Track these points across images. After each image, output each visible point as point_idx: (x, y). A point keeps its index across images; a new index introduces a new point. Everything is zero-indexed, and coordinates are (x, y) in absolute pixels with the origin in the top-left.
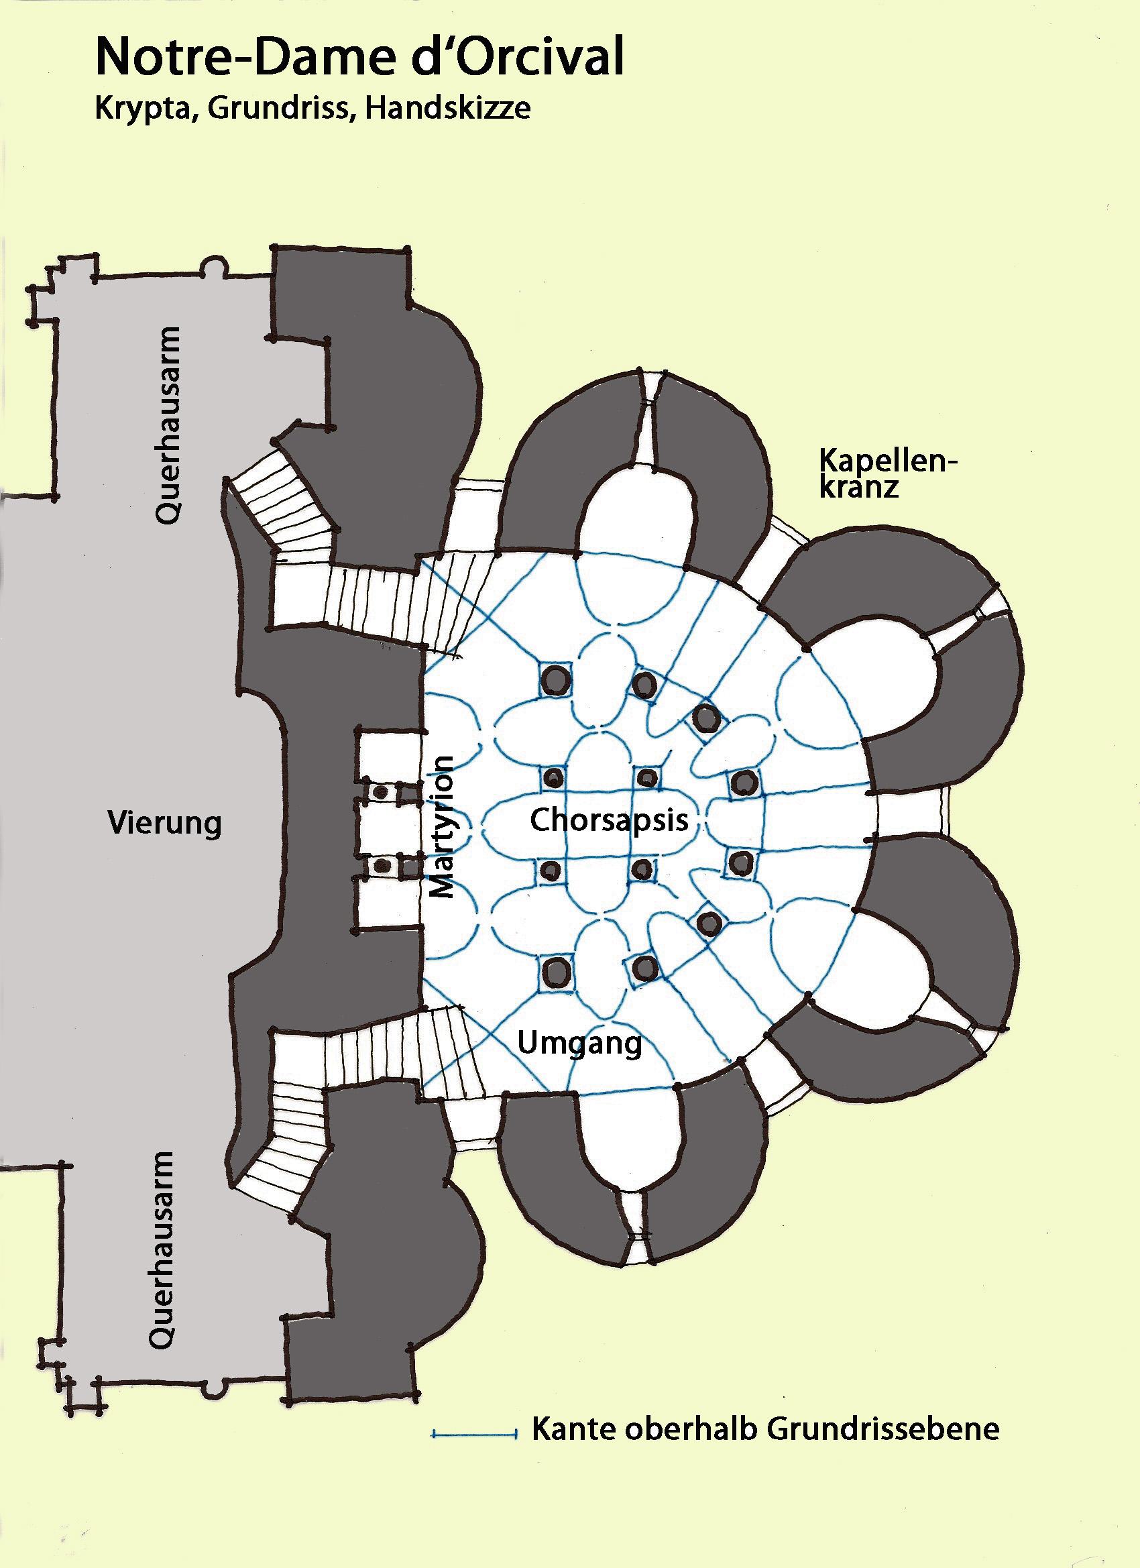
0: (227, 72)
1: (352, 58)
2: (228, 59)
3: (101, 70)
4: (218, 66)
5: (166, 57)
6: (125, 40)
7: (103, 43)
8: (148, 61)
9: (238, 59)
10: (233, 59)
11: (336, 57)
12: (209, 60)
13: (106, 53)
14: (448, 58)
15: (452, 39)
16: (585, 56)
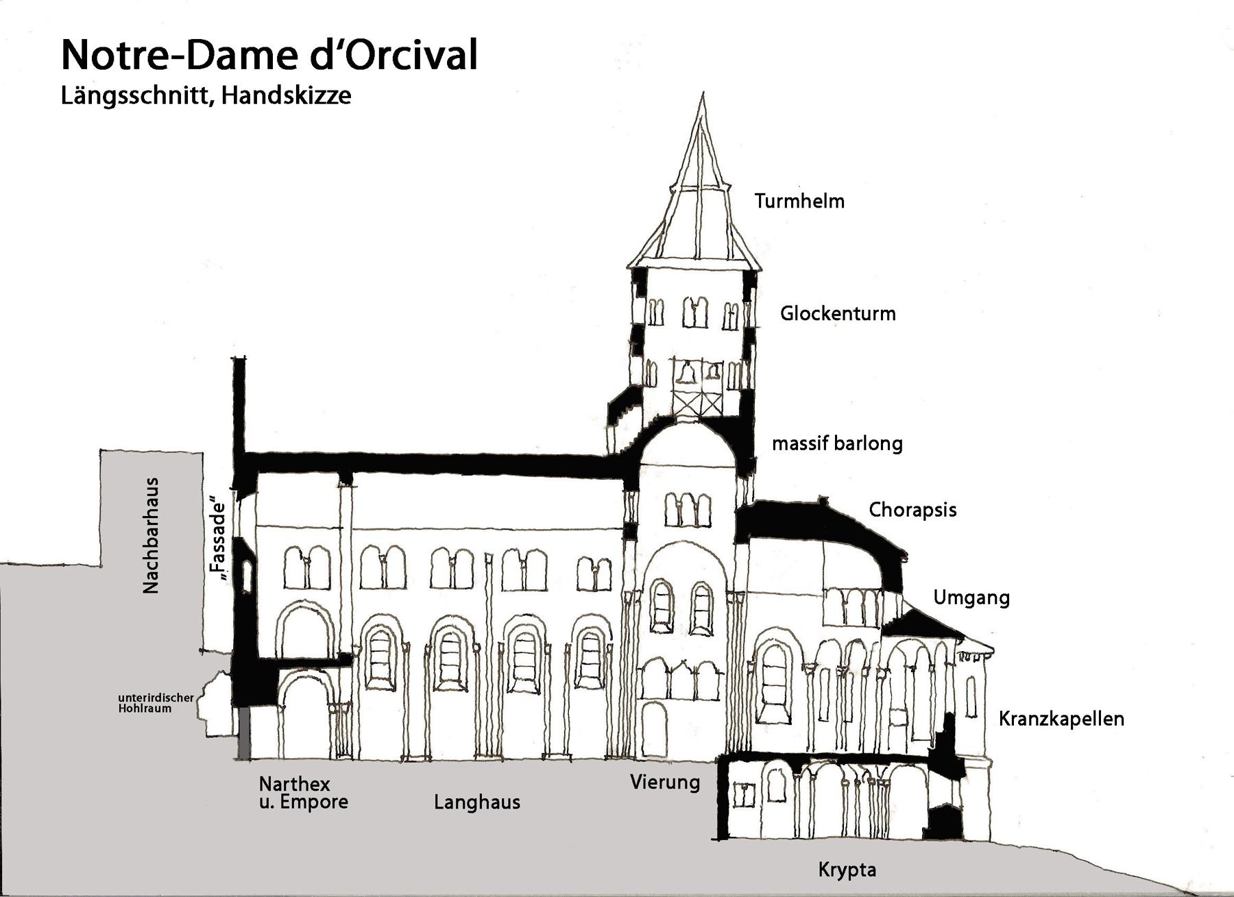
0: (165, 67)
1: (264, 56)
2: (165, 57)
4: (157, 62)
5: (117, 55)
6: (84, 42)
8: (103, 58)
9: (174, 57)
10: (170, 57)
11: (250, 56)
12: (151, 58)
13: (70, 53)
14: (339, 56)
15: (342, 41)
16: (447, 55)
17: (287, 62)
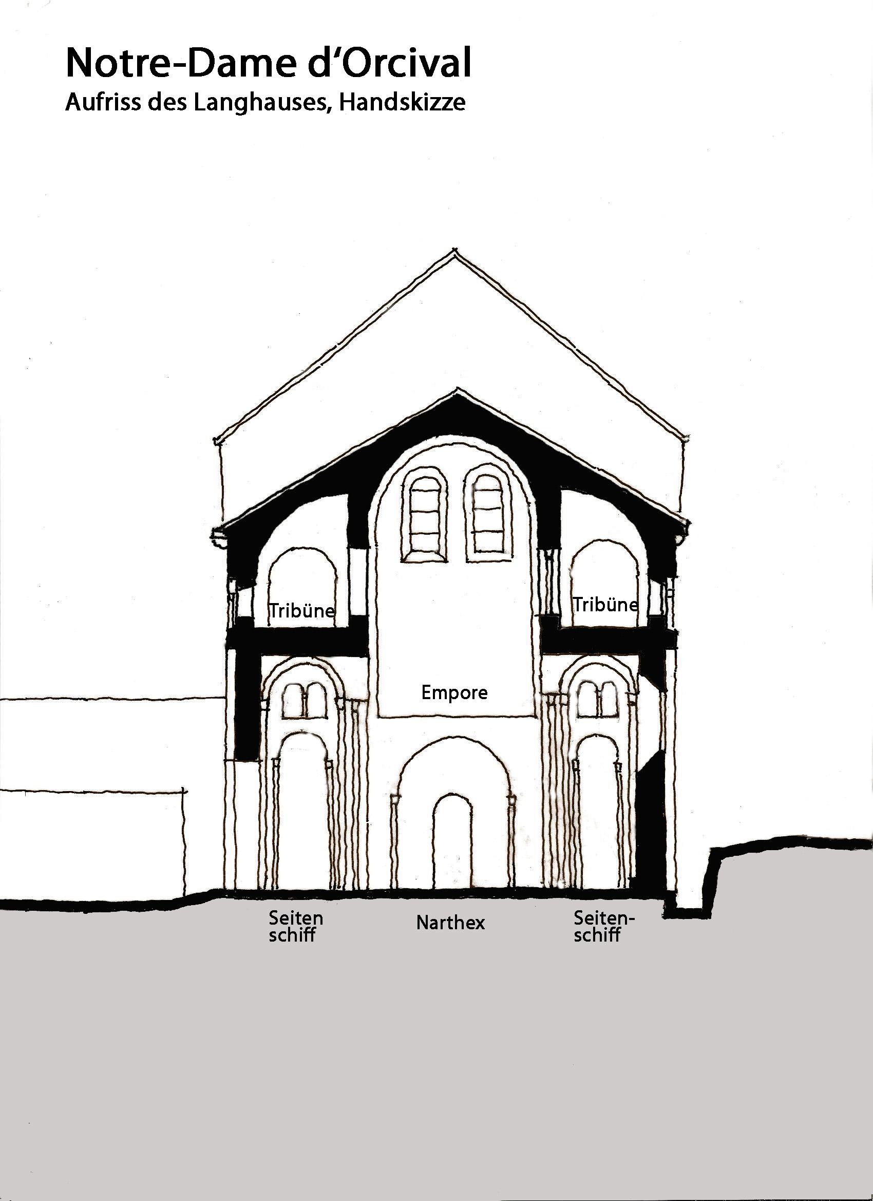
0: (166, 75)
1: (263, 64)
2: (167, 64)
3: (70, 73)
4: (159, 70)
5: (120, 63)
6: (88, 50)
7: (72, 53)
8: (106, 66)
9: (176, 65)
10: (172, 65)
11: (250, 64)
12: (153, 66)
14: (336, 64)
15: (339, 49)
16: (441, 63)
17: (286, 70)
